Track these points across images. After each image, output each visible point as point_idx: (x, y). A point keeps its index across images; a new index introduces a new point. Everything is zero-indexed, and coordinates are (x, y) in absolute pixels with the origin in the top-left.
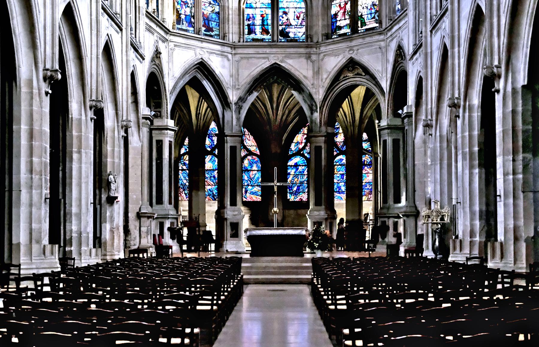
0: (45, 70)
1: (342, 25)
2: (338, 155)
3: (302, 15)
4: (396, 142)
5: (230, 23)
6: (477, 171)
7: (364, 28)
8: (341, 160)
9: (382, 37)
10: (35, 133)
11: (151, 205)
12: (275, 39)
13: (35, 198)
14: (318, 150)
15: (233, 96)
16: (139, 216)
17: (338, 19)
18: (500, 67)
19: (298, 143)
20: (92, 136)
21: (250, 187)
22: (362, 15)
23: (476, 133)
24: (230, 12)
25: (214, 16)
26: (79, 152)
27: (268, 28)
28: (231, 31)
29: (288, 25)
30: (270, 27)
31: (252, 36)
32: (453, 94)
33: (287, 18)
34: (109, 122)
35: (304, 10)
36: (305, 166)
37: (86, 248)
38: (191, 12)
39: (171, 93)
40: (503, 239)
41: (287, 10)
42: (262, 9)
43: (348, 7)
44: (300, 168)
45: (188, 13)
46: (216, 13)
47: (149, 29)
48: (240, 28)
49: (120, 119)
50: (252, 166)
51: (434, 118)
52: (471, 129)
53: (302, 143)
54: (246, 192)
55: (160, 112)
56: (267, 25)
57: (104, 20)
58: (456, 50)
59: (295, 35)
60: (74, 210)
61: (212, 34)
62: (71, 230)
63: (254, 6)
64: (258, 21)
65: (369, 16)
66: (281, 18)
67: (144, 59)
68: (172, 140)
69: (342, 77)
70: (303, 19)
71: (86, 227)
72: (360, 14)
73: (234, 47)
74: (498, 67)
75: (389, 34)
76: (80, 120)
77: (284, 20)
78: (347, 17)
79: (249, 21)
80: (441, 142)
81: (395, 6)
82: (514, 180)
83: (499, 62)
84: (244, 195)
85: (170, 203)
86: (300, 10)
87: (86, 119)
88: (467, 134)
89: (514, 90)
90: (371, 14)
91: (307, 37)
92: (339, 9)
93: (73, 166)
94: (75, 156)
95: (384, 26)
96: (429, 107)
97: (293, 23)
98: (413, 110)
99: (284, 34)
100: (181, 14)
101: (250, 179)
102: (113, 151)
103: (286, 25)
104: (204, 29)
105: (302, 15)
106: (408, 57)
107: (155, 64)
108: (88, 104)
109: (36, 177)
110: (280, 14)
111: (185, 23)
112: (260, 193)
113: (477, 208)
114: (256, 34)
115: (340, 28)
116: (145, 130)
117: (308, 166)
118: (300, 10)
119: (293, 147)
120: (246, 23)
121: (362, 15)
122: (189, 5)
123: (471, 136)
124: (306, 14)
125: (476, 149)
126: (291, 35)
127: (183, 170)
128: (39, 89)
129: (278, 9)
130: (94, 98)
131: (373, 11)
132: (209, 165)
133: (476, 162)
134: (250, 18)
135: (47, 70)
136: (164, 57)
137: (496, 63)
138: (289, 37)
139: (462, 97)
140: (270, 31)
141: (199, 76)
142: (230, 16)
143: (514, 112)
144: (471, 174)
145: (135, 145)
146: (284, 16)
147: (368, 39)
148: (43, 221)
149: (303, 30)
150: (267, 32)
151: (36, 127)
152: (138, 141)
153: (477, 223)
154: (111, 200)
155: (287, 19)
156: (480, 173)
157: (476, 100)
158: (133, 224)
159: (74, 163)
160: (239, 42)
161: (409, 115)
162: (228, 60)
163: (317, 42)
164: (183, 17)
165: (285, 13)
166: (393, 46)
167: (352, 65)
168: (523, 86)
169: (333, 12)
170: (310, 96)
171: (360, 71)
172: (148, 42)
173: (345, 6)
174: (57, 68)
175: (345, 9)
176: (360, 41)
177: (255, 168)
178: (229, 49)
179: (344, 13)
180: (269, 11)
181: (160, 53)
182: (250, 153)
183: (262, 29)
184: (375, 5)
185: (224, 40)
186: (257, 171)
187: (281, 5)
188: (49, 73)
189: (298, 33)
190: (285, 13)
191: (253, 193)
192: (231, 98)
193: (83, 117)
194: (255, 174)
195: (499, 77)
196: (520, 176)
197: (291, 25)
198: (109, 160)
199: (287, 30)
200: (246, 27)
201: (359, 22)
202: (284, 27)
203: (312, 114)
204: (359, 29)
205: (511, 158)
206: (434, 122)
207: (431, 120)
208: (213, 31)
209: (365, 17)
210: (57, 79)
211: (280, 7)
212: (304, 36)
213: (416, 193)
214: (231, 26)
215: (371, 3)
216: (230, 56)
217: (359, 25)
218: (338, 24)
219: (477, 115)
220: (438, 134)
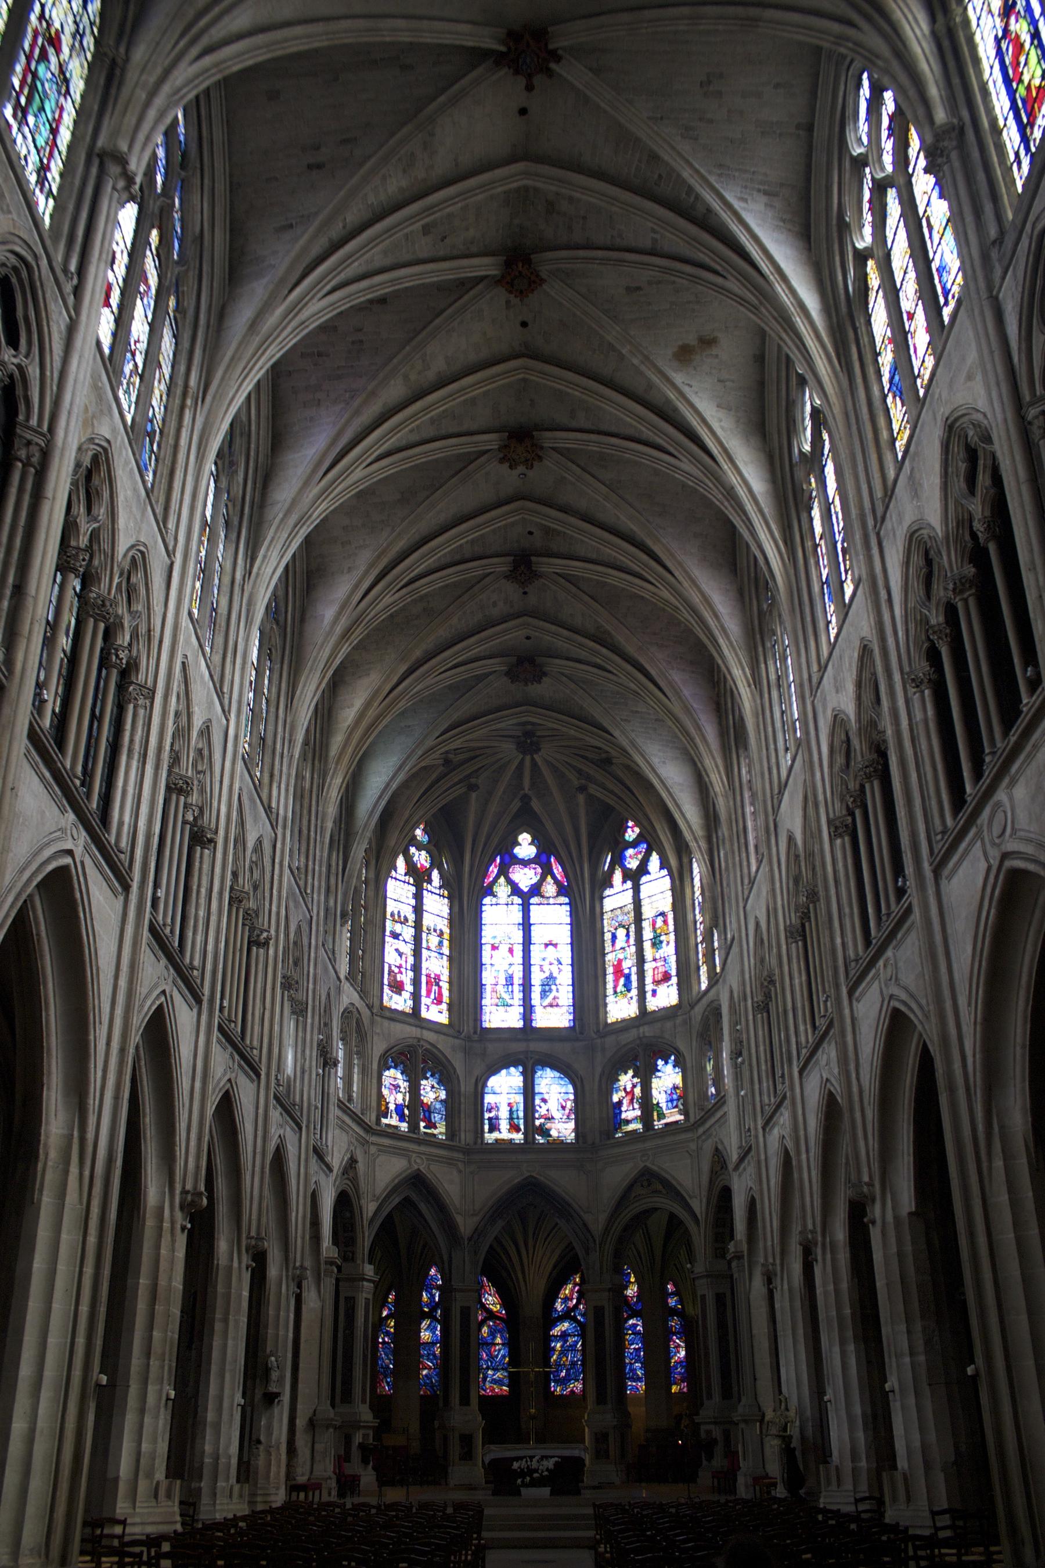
0: (184, 1192)
1: (629, 1118)
2: (630, 1317)
4: (720, 1299)
5: (462, 1116)
6: (851, 1347)
7: (663, 1122)
8: (635, 1325)
9: (689, 1135)
10: (161, 1290)
11: (333, 1406)
12: (530, 1137)
13: (151, 1399)
14: (598, 1313)
15: (465, 1225)
16: (312, 1424)
17: (624, 1108)
18: (873, 1185)
19: (567, 1299)
20: (246, 1294)
21: (490, 1372)
22: (658, 1103)
23: (844, 1286)
24: (462, 1100)
25: (438, 1106)
26: (226, 1320)
28: (463, 1128)
29: (549, 1119)
30: (522, 1122)
31: (495, 1135)
32: (805, 1225)
34: (273, 1271)
35: (572, 1097)
36: (578, 1335)
37: (224, 1484)
38: (404, 1100)
39: (371, 1221)
40: (906, 1466)
41: (546, 1096)
42: (510, 1096)
43: (638, 1091)
44: (571, 1340)
45: (400, 1101)
46: (441, 1101)
47: (342, 1126)
48: (476, 1123)
49: (291, 1265)
50: (494, 1338)
51: (778, 1262)
52: (836, 1282)
53: (572, 1299)
54: (485, 1379)
55: (353, 1253)
56: (518, 1118)
57: (276, 1114)
58: (804, 1156)
60: (210, 1416)
61: (435, 1132)
62: (204, 1452)
63: (498, 1090)
64: (504, 1114)
65: (670, 1104)
67: (331, 1170)
68: (370, 1297)
69: (633, 1195)
71: (228, 1446)
72: (655, 1102)
73: (467, 1151)
74: (870, 1184)
75: (701, 1130)
76: (230, 1268)
77: (543, 1111)
78: (636, 1106)
79: (490, 1111)
80: (791, 1300)
81: (707, 1089)
82: (912, 1364)
83: (871, 1177)
84: (481, 1384)
85: (364, 1401)
86: (566, 1097)
87: (240, 1267)
88: (831, 1287)
89: (897, 1218)
90: (672, 1101)
91: (577, 1137)
92: (624, 1094)
93: (215, 1344)
94: (218, 1326)
95: (692, 1120)
96: (769, 1243)
97: (557, 1114)
98: (745, 1247)
99: (545, 1132)
100: (388, 1103)
101: (491, 1357)
102: (278, 1316)
104: (422, 1124)
106: (731, 1167)
107: (348, 1179)
108: (244, 1243)
109: (154, 1363)
110: (537, 1101)
111: (394, 1115)
112: (506, 1381)
113: (858, 1410)
115: (628, 1122)
116: (328, 1284)
117: (583, 1335)
118: (566, 1097)
119: (559, 1306)
120: (487, 1115)
121: (658, 1103)
122: (402, 1090)
123: (837, 1291)
124: (575, 1101)
125: (848, 1311)
126: (554, 1133)
127: (384, 1342)
128: (173, 1222)
130: (253, 1234)
131: (675, 1097)
132: (425, 1335)
133: (850, 1334)
135: (188, 1192)
136: (361, 1166)
137: (866, 1179)
138: (550, 1136)
139: (819, 1229)
140: (522, 1127)
141: (414, 1197)
142: (463, 1106)
143: (900, 1254)
144: (843, 1354)
145: (312, 1305)
146: (542, 1104)
147: (668, 1140)
148: (160, 1440)
149: (572, 1125)
150: (518, 1130)
151: (162, 1282)
152: (316, 1302)
153: (860, 1435)
154: (271, 1399)
156: (857, 1351)
157: (840, 1233)
158: (302, 1441)
159: (215, 1338)
160: (475, 1143)
161: (739, 1257)
162: (460, 1171)
163: (593, 1143)
164: (392, 1107)
165: (544, 1101)
166: (708, 1147)
167: (648, 1178)
168: (910, 1214)
169: (615, 1098)
170: (585, 1225)
171: (660, 1187)
172: (338, 1146)
173: (632, 1090)
174: (203, 1189)
175: (633, 1095)
176: (659, 1142)
177: (498, 1340)
178: (461, 1156)
179: (631, 1101)
180: (520, 1099)
181: (356, 1162)
182: (491, 1315)
183: (510, 1125)
184: (678, 1088)
185: (452, 1140)
186: (503, 1344)
188: (189, 1198)
191: (494, 1381)
192: (462, 1230)
193: (235, 1264)
194: (500, 1350)
195: (873, 1200)
196: (922, 1358)
197: (553, 1118)
198: (271, 1331)
199: (548, 1126)
200: (486, 1122)
201: (655, 1114)
202: (542, 1120)
203: (588, 1254)
204: (656, 1123)
205: (903, 1327)
206: (778, 1268)
207: (774, 1264)
208: (435, 1128)
209: (663, 1105)
210: (201, 1206)
212: (573, 1134)
213: (758, 1382)
214: (463, 1121)
215: (671, 1086)
216: (461, 1165)
217: (655, 1117)
218: (624, 1116)
219: (843, 1257)
220: (786, 1287)
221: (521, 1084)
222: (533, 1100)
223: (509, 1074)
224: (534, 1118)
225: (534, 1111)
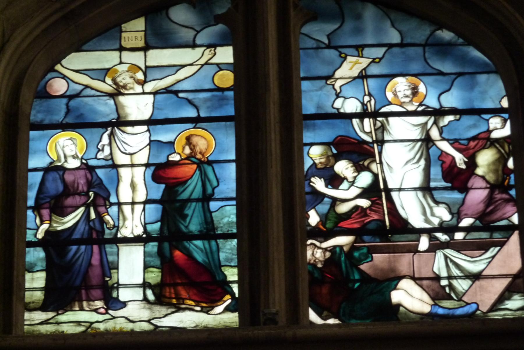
3: (485, 158)
27: (213, 255)
29: (380, 232)
30: (229, 249)
33: (365, 179)
42: (165, 135)
56: (210, 232)
59: (438, 295)
63: (105, 109)
66: (319, 184)
70: (496, 187)
86: (469, 127)
103: (358, 233)
105: (485, 158)
110: (315, 154)
114: (113, 303)
118: (469, 127)
126: (410, 297)
129: (293, 121)
134: (69, 190)
146: (343, 168)
150: (207, 289)
155: (375, 191)
183: (166, 263)
187: (312, 98)
189: (462, 285)
190: (361, 154)
197: (401, 226)
211: (309, 107)
221: (227, 78)
222: (293, 150)
223: (159, 37)
224: (298, 234)
225: (297, 195)
